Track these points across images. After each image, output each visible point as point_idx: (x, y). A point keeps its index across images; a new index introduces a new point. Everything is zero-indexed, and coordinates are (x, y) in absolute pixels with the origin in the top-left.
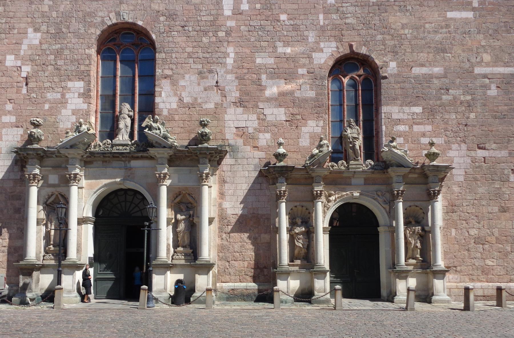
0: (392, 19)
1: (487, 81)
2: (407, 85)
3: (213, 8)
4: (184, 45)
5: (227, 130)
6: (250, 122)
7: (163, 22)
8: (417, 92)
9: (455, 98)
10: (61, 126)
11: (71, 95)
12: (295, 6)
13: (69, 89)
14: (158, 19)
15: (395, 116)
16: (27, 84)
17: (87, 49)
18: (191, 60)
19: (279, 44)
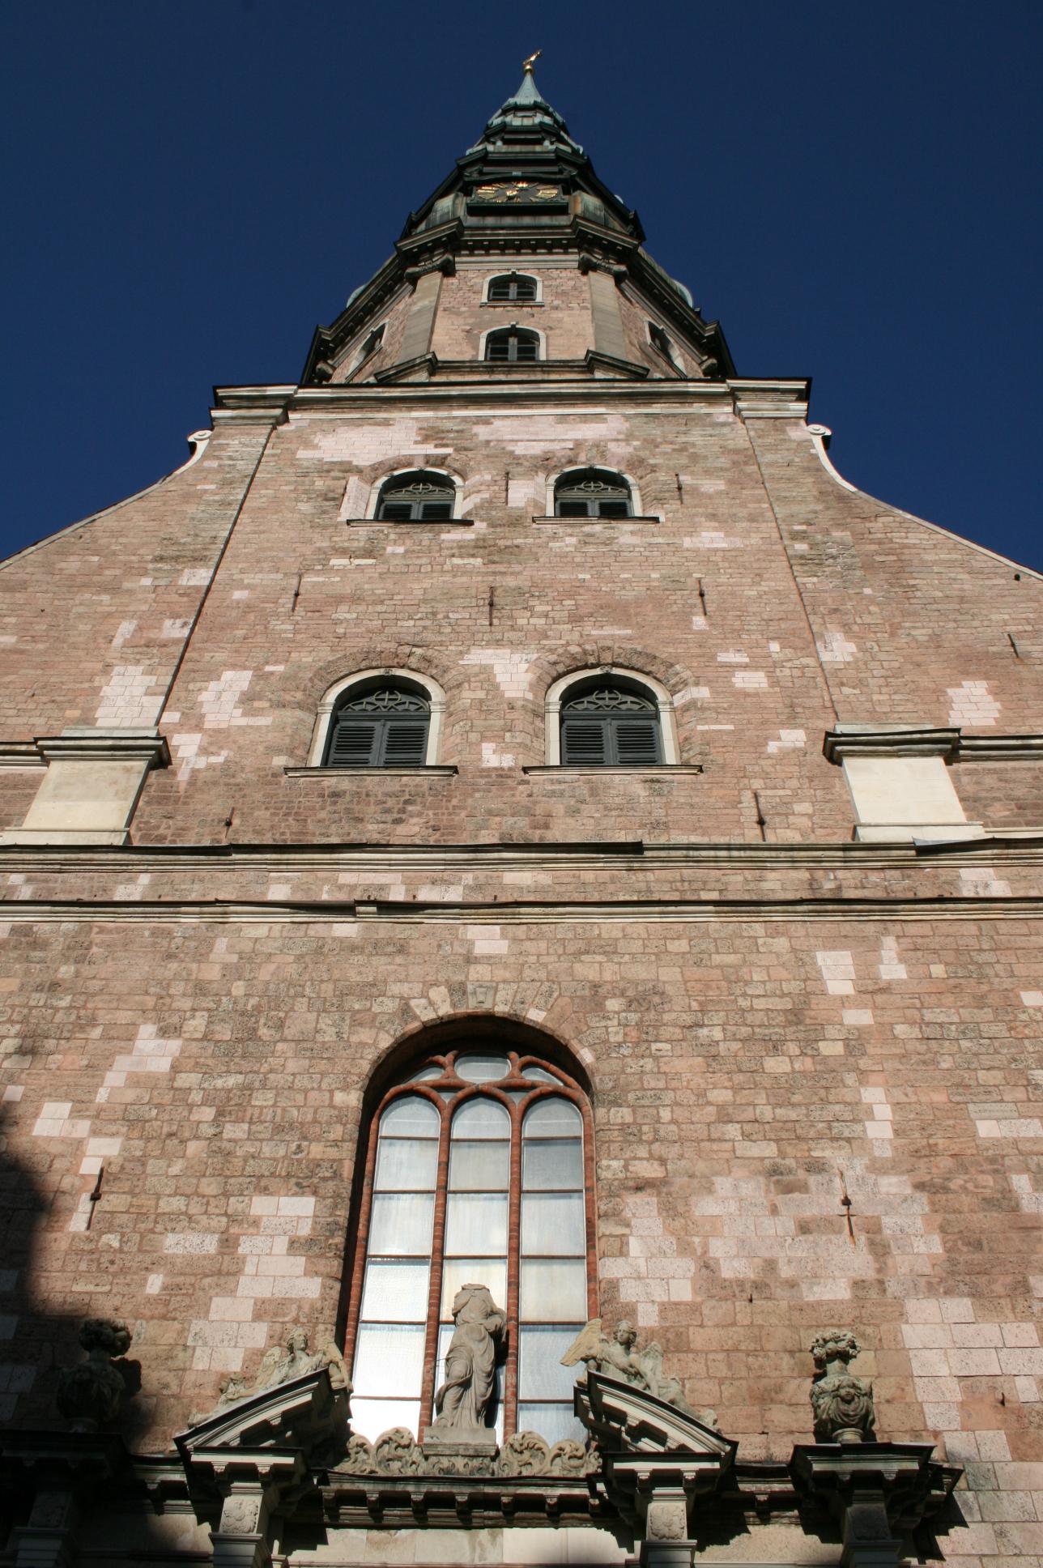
3: (784, 974)
4: (698, 1081)
5: (922, 1391)
7: (618, 1013)
10: (201, 1362)
13: (256, 1223)
14: (599, 1006)
16: (95, 1197)
17: (343, 1089)
18: (733, 1131)
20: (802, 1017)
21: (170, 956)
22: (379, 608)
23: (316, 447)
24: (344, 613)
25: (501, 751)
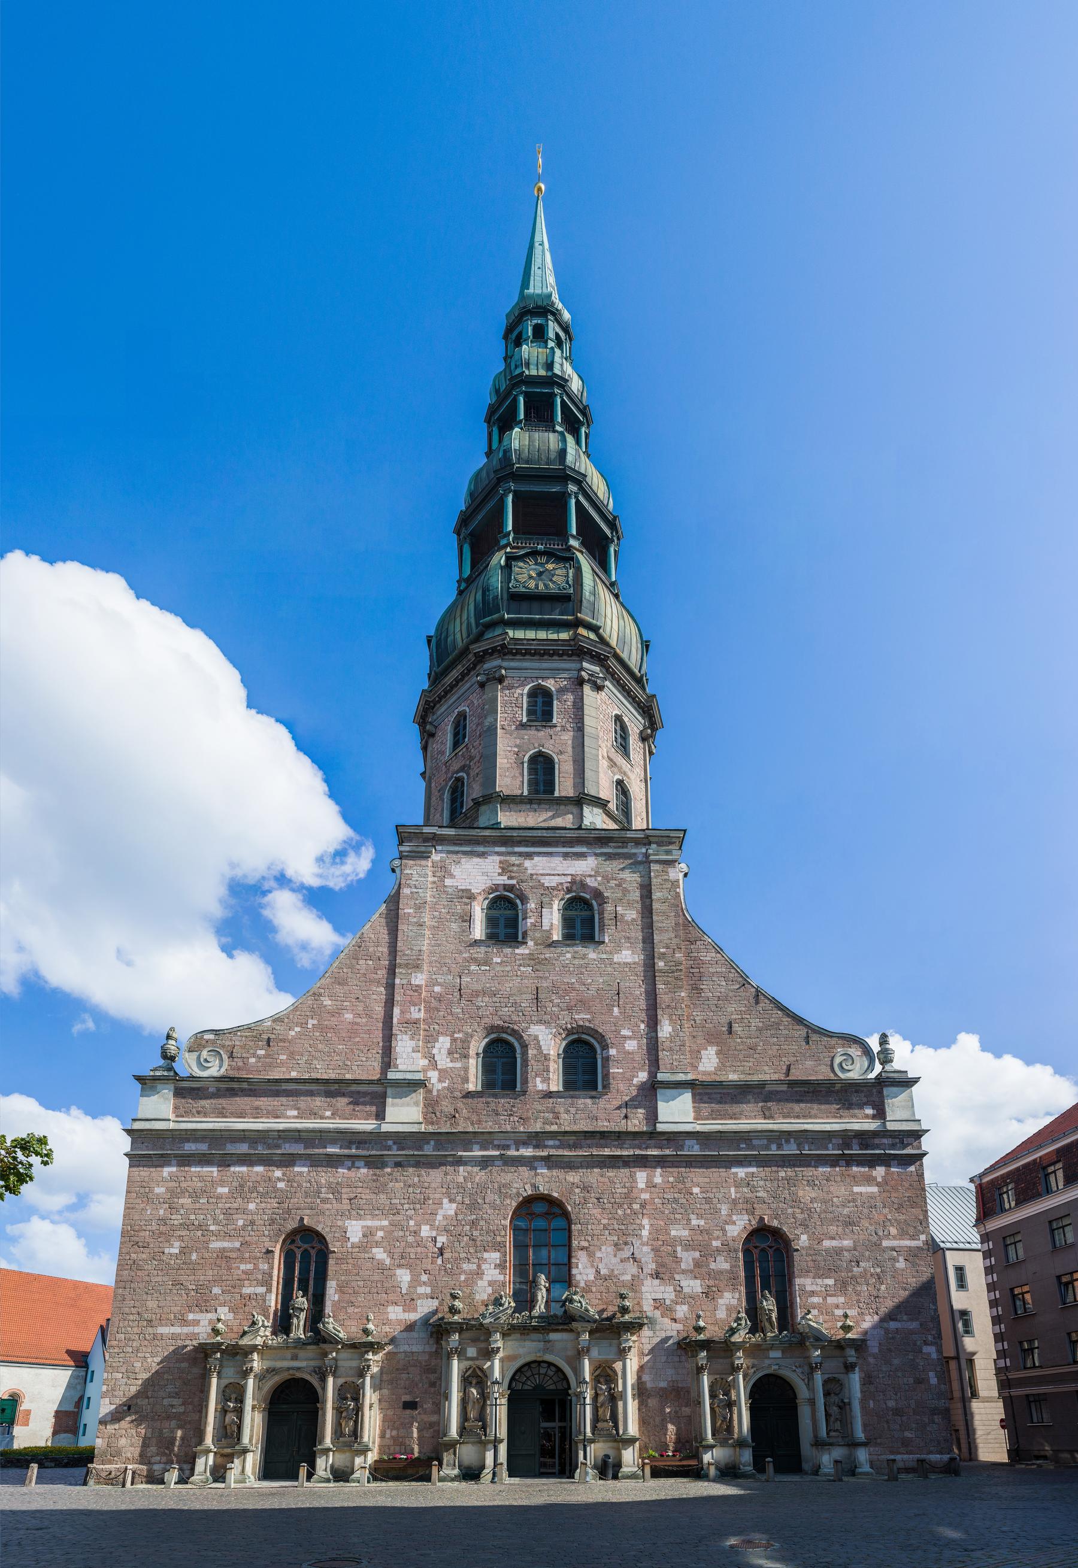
0: (801, 1193)
1: (895, 1253)
2: (819, 1258)
6: (668, 1293)
8: (829, 1265)
9: (865, 1270)
11: (487, 1266)
12: (707, 1180)
15: (808, 1288)
18: (607, 1232)
19: (692, 1216)
20: (629, 1196)
21: (446, 1174)
22: (495, 999)
23: (452, 876)
24: (480, 1002)
25: (542, 1082)
